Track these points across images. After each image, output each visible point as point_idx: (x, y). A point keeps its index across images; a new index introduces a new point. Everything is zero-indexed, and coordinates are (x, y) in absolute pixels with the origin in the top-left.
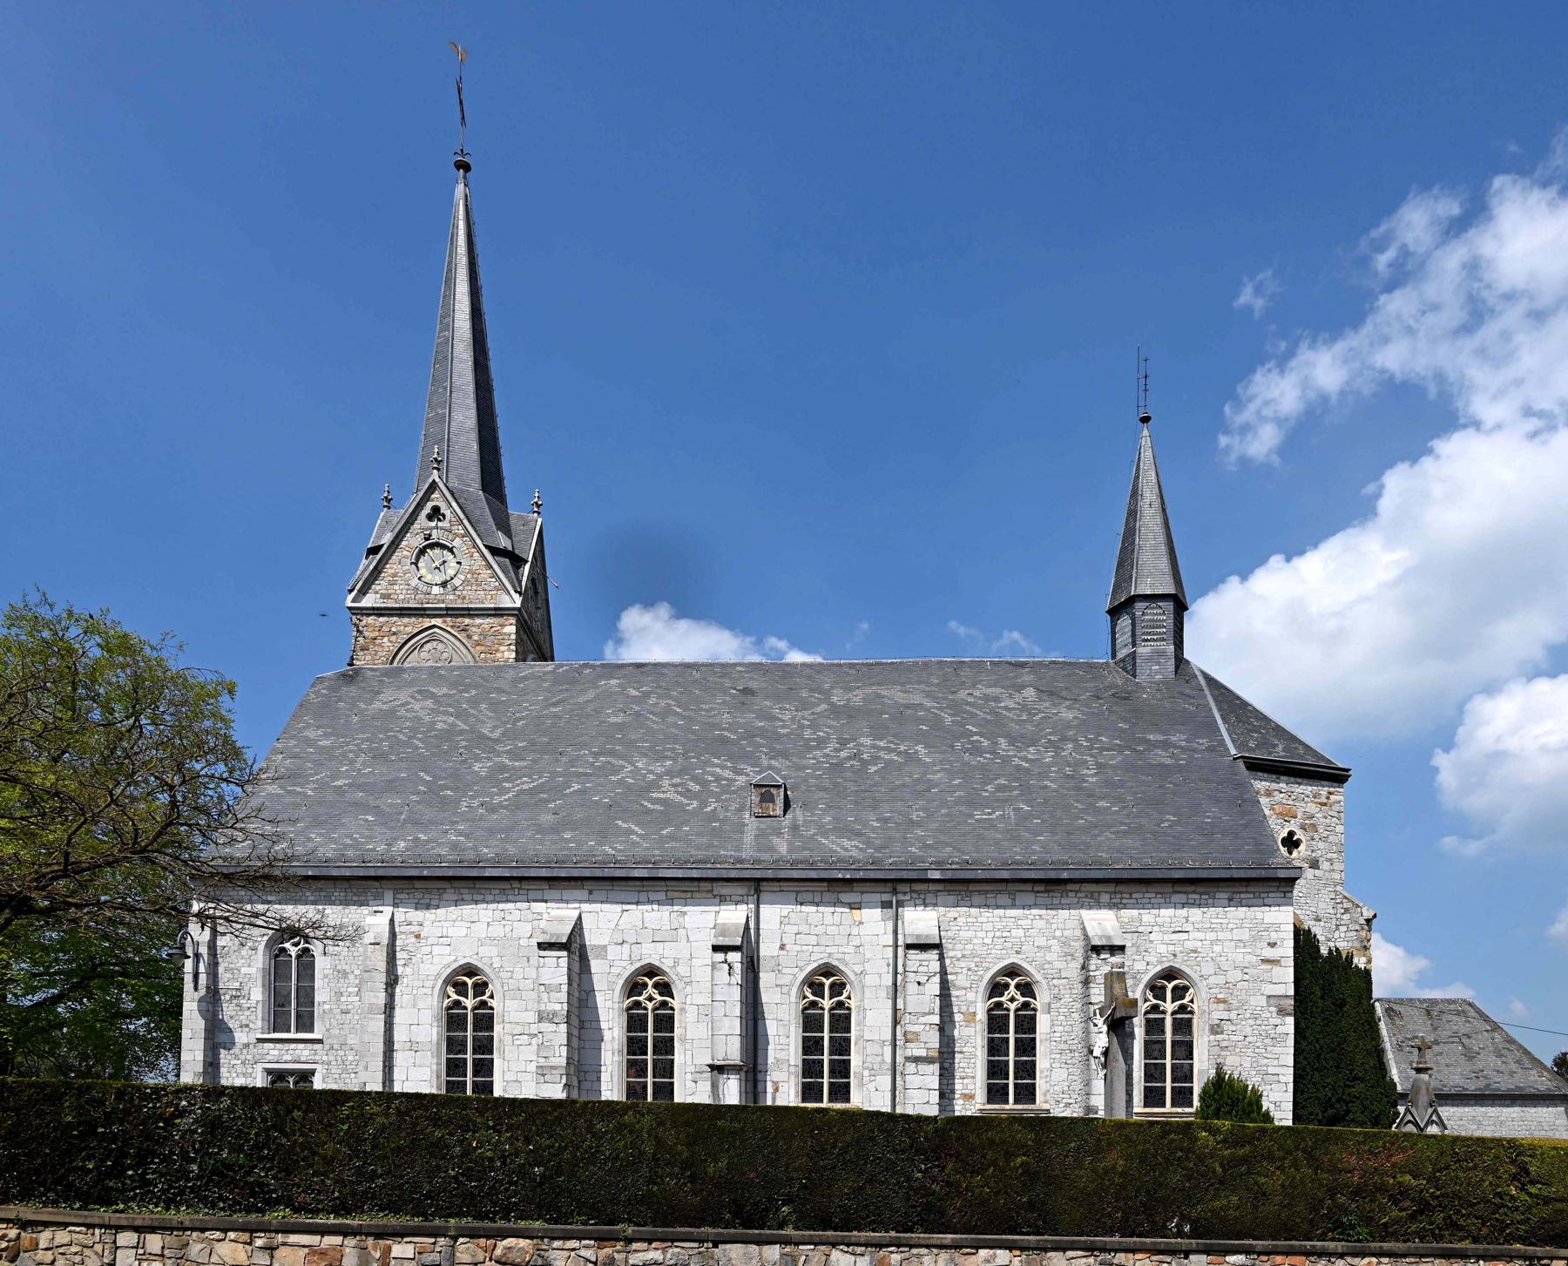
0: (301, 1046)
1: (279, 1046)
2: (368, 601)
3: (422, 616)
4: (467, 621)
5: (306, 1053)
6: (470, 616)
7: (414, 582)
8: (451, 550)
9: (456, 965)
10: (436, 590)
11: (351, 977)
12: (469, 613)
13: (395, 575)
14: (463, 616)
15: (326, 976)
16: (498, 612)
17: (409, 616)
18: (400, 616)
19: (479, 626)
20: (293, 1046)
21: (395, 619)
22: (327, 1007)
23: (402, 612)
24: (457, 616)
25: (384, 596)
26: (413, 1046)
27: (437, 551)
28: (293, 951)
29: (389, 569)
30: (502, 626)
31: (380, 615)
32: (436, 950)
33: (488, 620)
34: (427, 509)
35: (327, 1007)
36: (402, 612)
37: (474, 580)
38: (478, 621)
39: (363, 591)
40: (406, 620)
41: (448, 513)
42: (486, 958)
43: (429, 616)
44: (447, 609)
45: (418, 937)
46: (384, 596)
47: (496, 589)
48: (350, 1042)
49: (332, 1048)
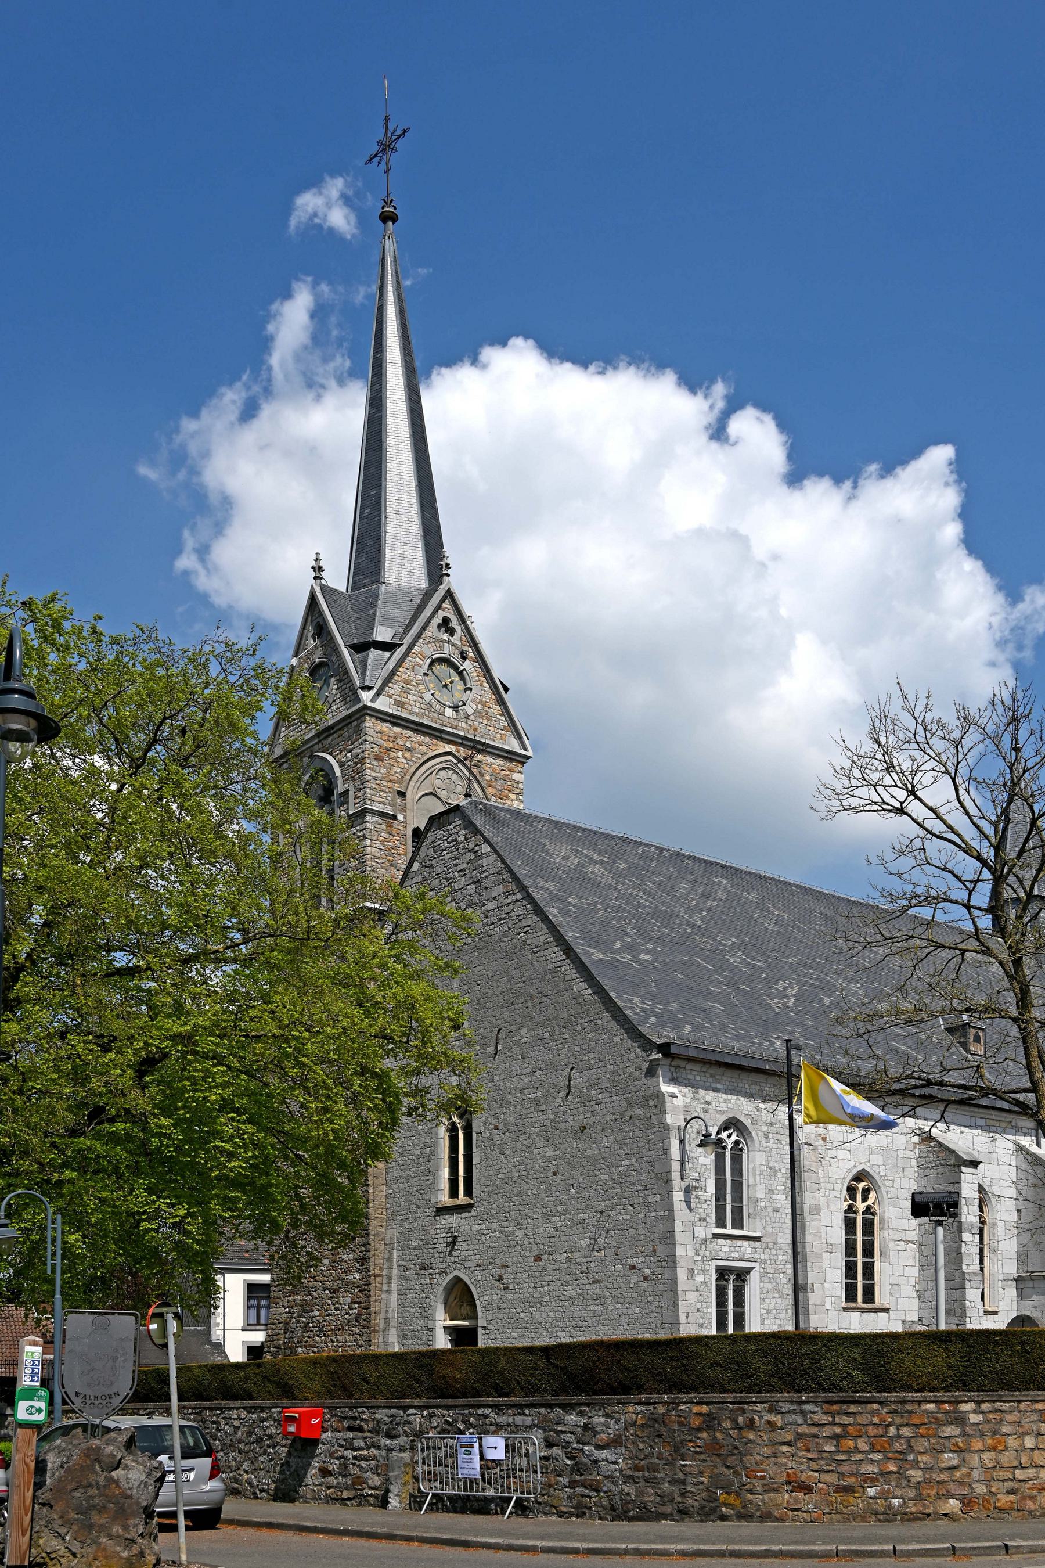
0: (746, 1243)
1: (729, 1242)
2: (383, 704)
3: (437, 738)
5: (749, 1250)
8: (460, 674)
9: (855, 1171)
10: (449, 712)
11: (779, 1175)
12: (483, 748)
13: (408, 682)
15: (762, 1172)
17: (424, 734)
18: (415, 731)
20: (739, 1243)
21: (409, 733)
22: (763, 1204)
23: (419, 728)
25: (400, 704)
26: (829, 1248)
27: (444, 667)
28: (729, 1143)
29: (403, 674)
30: (512, 771)
31: (395, 724)
32: (841, 1154)
33: (498, 761)
34: (438, 620)
35: (763, 1204)
36: (419, 728)
38: (490, 760)
40: (420, 738)
41: (458, 629)
42: (876, 1165)
43: (443, 740)
44: (464, 738)
45: (824, 1139)
48: (780, 1241)
49: (767, 1247)
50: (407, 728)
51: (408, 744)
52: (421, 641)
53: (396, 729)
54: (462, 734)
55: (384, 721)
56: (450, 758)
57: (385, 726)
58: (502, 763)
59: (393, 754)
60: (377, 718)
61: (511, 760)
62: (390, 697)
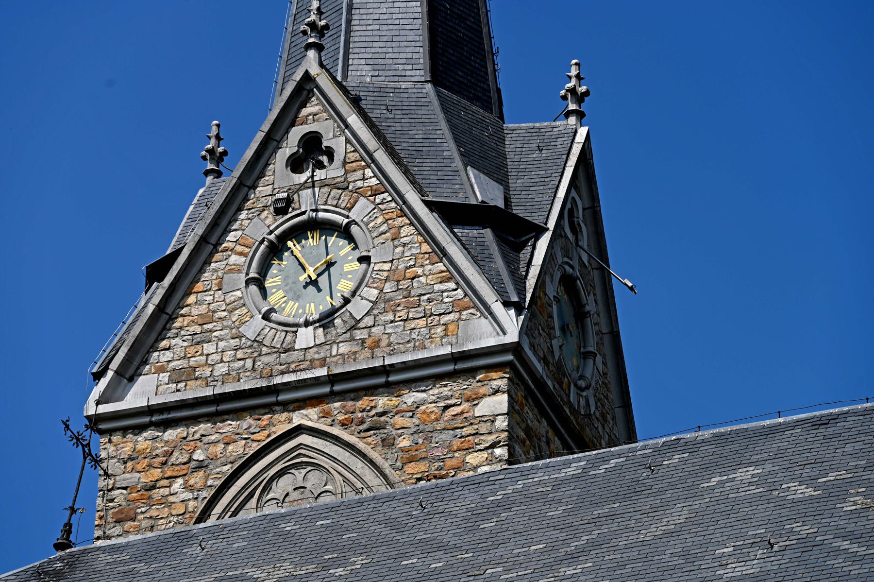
3: (269, 408)
4: (382, 402)
6: (390, 388)
7: (255, 326)
10: (306, 337)
13: (207, 318)
14: (371, 391)
16: (463, 365)
17: (237, 414)
18: (213, 418)
19: (413, 410)
21: (203, 427)
24: (356, 394)
29: (195, 306)
30: (474, 399)
31: (166, 425)
37: (401, 297)
38: (411, 397)
39: (129, 373)
40: (229, 426)
46: (180, 376)
47: (458, 307)
50: (195, 420)
51: (199, 455)
52: (243, 215)
53: (171, 434)
54: (322, 372)
55: (139, 429)
56: (305, 439)
57: (143, 441)
58: (445, 391)
59: (157, 494)
60: (125, 430)
61: (472, 372)
62: (161, 370)
